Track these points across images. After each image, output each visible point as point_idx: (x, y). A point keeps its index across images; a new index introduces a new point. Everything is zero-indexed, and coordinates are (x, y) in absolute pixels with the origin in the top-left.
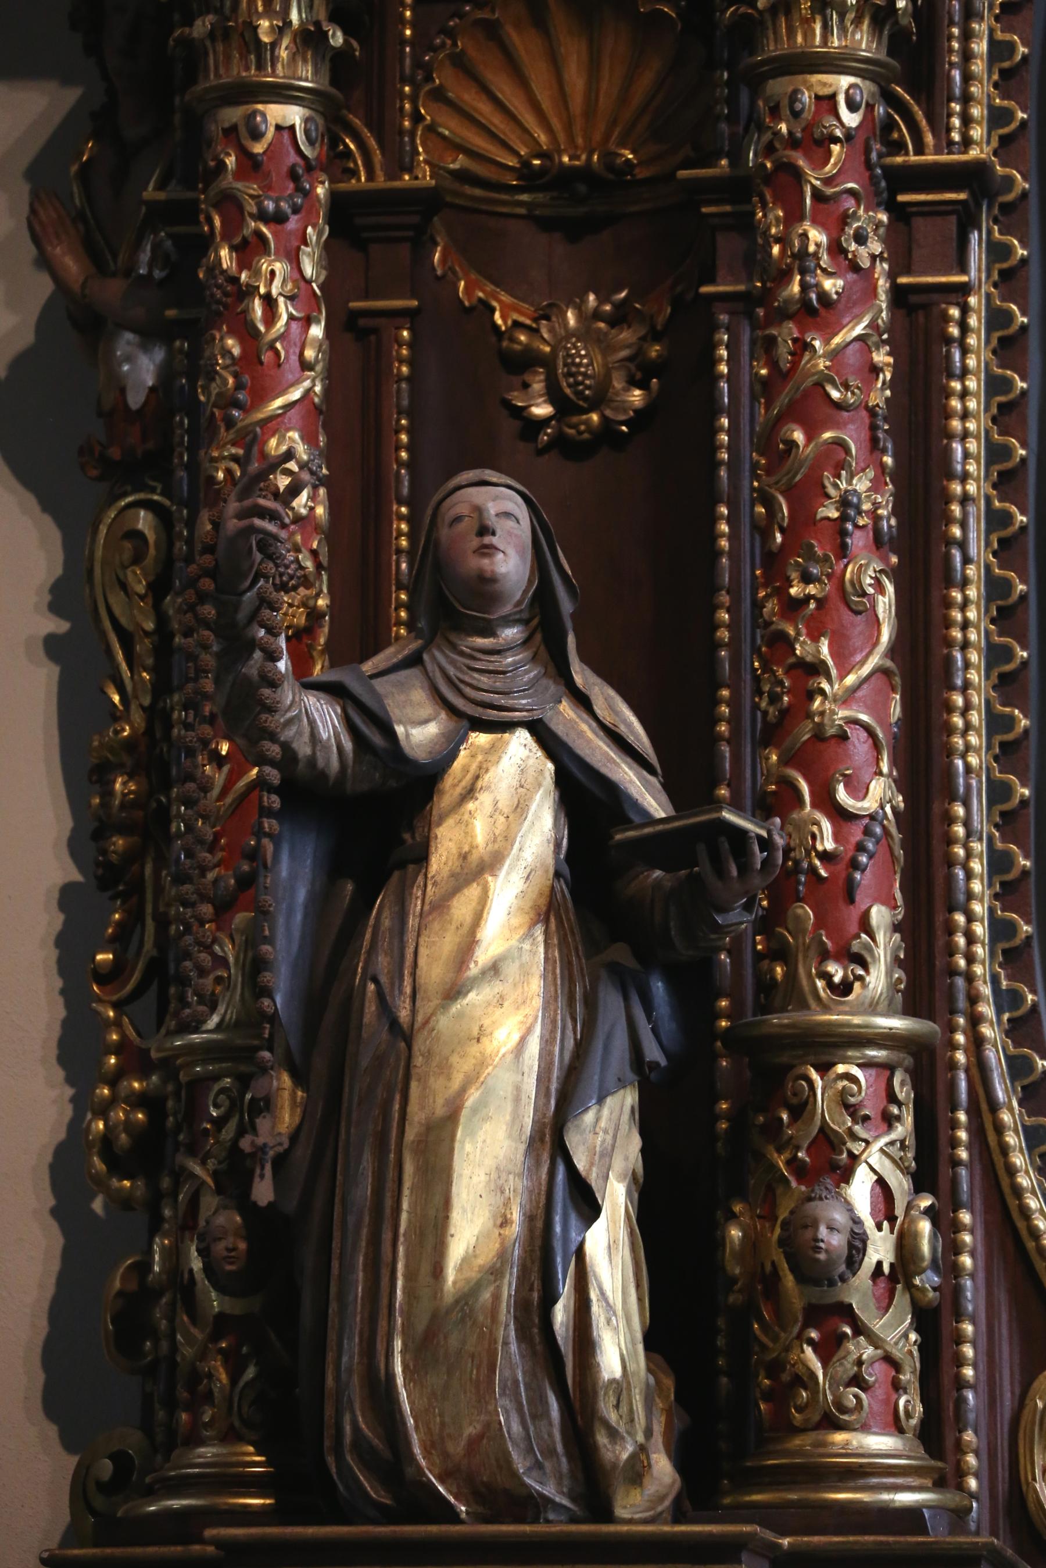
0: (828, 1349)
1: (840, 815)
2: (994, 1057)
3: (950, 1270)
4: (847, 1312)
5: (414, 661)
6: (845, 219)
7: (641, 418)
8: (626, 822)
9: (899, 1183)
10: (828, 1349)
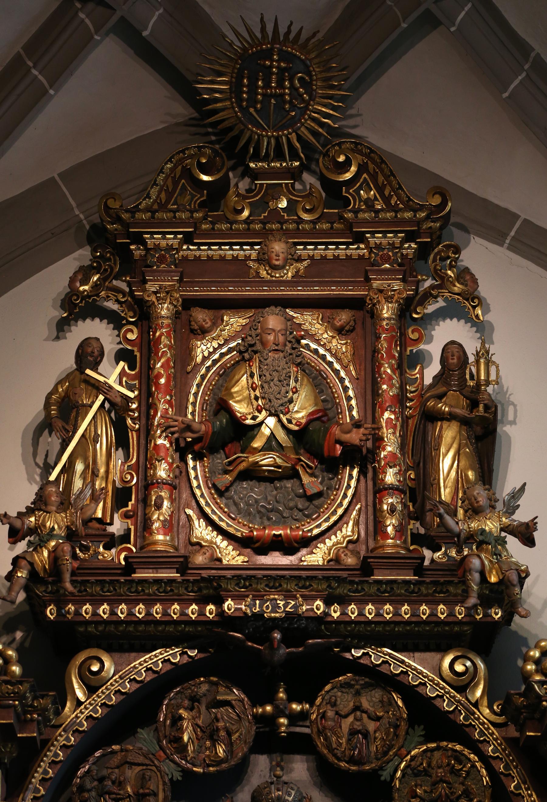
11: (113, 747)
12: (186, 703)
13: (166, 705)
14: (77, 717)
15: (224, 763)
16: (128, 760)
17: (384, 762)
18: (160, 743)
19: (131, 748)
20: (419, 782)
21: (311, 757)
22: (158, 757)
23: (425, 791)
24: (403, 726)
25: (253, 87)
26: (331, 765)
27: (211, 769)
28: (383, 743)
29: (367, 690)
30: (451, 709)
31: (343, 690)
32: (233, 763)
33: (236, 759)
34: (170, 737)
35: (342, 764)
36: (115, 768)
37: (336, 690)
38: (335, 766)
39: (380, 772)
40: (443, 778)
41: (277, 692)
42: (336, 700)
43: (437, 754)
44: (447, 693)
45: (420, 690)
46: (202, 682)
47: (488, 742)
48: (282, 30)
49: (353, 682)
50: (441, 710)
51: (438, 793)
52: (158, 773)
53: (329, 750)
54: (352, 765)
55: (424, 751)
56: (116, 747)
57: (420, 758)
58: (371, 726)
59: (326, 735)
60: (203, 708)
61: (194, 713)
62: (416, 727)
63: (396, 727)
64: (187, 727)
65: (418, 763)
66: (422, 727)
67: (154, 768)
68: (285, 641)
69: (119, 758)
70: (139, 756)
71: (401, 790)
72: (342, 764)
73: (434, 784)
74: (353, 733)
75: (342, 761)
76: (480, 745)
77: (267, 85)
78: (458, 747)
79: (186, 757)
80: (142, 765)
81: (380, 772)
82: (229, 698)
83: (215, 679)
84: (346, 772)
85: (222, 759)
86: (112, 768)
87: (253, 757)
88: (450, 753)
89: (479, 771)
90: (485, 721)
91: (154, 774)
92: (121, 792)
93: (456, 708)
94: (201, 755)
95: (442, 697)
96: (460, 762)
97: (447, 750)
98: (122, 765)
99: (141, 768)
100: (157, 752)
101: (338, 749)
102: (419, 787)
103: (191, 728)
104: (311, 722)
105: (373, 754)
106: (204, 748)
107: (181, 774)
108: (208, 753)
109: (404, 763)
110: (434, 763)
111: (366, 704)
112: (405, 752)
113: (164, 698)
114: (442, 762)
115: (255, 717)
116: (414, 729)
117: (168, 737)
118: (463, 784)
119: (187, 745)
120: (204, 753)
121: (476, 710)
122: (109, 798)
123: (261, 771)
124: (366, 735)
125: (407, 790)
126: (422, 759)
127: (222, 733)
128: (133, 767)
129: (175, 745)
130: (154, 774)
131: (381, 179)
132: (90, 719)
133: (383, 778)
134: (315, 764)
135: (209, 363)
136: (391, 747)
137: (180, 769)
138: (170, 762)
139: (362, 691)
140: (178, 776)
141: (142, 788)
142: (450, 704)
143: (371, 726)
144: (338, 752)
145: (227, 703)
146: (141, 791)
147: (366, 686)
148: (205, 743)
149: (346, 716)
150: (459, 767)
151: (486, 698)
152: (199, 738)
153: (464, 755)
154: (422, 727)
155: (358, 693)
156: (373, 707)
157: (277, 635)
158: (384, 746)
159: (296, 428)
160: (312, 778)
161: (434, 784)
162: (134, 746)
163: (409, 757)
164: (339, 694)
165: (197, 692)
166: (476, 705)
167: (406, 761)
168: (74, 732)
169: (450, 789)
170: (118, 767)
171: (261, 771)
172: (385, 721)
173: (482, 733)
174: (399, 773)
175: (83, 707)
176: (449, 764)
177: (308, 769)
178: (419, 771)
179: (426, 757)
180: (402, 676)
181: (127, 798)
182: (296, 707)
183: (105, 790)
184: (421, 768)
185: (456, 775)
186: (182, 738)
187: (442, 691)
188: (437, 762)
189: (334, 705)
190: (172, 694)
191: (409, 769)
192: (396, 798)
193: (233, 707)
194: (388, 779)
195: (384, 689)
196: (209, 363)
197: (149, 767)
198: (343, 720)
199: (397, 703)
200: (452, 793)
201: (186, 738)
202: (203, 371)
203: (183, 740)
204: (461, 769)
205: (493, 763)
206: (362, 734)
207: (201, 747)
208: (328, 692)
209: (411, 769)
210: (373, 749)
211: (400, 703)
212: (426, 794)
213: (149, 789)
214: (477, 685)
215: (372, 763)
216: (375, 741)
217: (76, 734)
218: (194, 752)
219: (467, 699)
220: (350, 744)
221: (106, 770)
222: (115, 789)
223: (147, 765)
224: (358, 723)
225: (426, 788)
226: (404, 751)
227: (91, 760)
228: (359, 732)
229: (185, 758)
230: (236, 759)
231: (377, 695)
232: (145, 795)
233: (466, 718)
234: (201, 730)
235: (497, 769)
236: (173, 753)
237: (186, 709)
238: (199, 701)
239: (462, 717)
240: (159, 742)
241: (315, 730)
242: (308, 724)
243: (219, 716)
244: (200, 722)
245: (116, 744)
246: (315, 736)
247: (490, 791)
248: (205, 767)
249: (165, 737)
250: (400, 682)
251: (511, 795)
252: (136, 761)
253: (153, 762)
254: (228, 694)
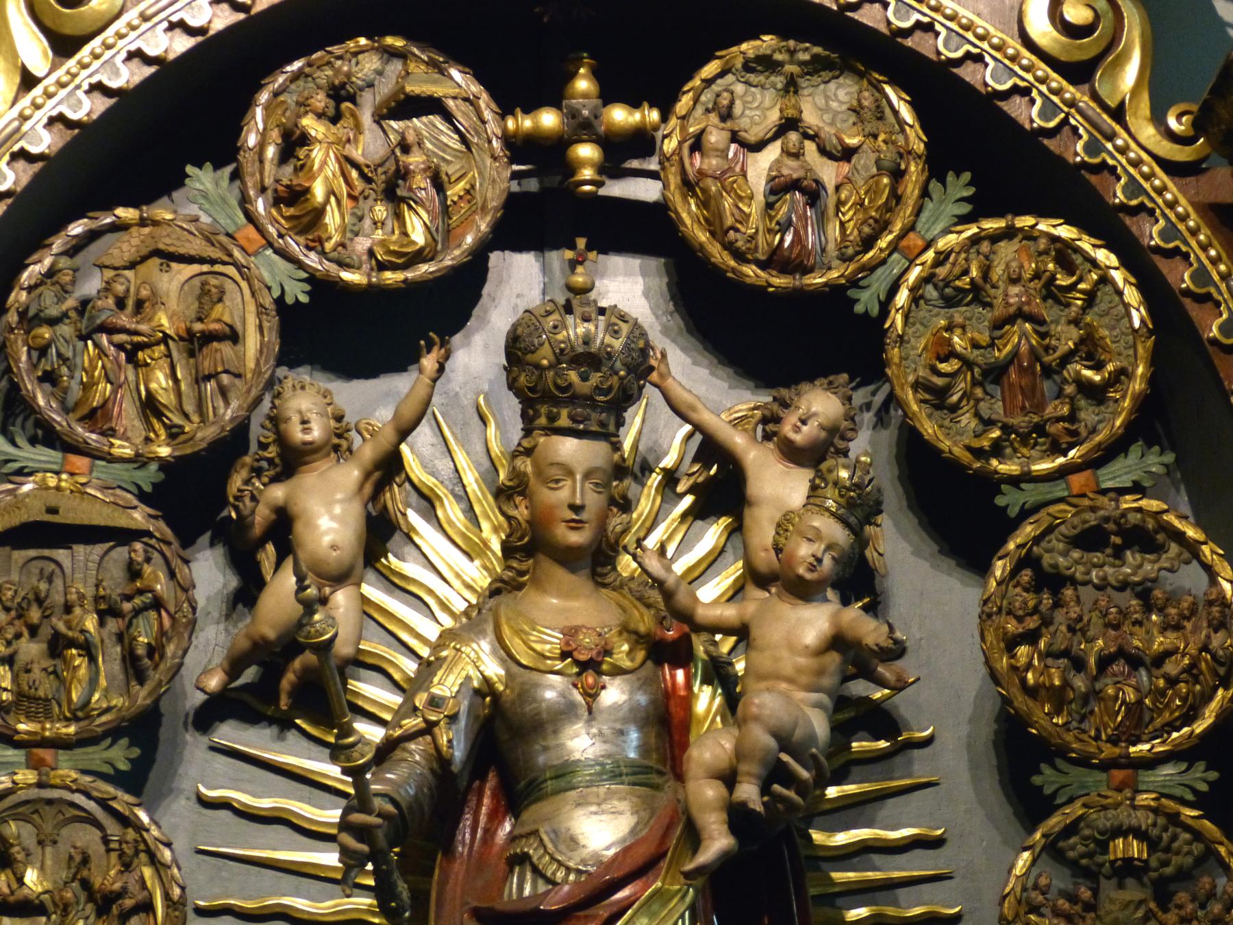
11: (120, 212)
12: (320, 100)
13: (267, 108)
14: (24, 118)
15: (425, 261)
16: (161, 246)
17: (862, 268)
18: (248, 206)
19: (169, 216)
20: (958, 319)
21: (655, 263)
22: (243, 242)
23: (975, 345)
24: (915, 171)
26: (717, 272)
27: (388, 275)
28: (861, 216)
29: (816, 79)
30: (1052, 124)
31: (752, 77)
32: (448, 262)
33: (457, 252)
34: (276, 191)
35: (750, 271)
36: (125, 268)
37: (730, 78)
38: (730, 275)
39: (851, 293)
40: (1026, 308)
41: (573, 75)
42: (732, 103)
43: (1007, 250)
44: (1042, 81)
45: (967, 73)
46: (362, 51)
47: (1151, 212)
49: (778, 57)
50: (1020, 127)
51: (1009, 348)
52: (244, 284)
53: (713, 234)
54: (774, 273)
55: (975, 240)
56: (126, 213)
57: (963, 255)
58: (829, 173)
59: (705, 191)
60: (366, 118)
61: (343, 129)
62: (950, 177)
63: (898, 175)
64: (324, 163)
65: (957, 270)
66: (967, 176)
67: (231, 270)
69: (135, 241)
70: (191, 237)
71: (908, 342)
72: (750, 271)
73: (998, 325)
74: (779, 188)
75: (748, 262)
76: (1128, 221)
78: (1066, 232)
79: (320, 241)
80: (201, 261)
81: (850, 293)
82: (438, 90)
83: (399, 43)
84: (759, 292)
85: (422, 250)
86: (116, 269)
87: (495, 258)
88: (1043, 243)
89: (1120, 293)
90: (1145, 156)
91: (234, 285)
92: (143, 327)
93: (1065, 122)
94: (359, 239)
95: (1025, 92)
96: (1069, 268)
97: (1035, 239)
98: (144, 259)
99: (196, 268)
100: (239, 229)
101: (737, 230)
102: (958, 331)
103: (333, 166)
104: (665, 160)
105: (831, 247)
106: (367, 223)
107: (307, 287)
108: (379, 235)
109: (919, 269)
110: (998, 272)
111: (810, 118)
112: (920, 243)
113: (259, 87)
114: (1021, 267)
115: (509, 140)
116: (943, 181)
117: (270, 192)
118: (1076, 322)
119: (320, 212)
120: (368, 236)
121: (1118, 128)
122: (111, 342)
123: (518, 296)
124: (814, 194)
125: (923, 342)
126: (966, 259)
127: (421, 182)
128: (174, 265)
129: (291, 211)
130: (229, 285)
132: (59, 126)
133: (859, 308)
134: (666, 280)
136: (882, 226)
137: (305, 275)
138: (276, 257)
139: (803, 82)
140: (298, 292)
141: (200, 320)
142: (1049, 110)
143: (829, 173)
144: (738, 236)
145: (433, 106)
146: (198, 327)
147: (816, 67)
148: (371, 210)
149: (758, 147)
150: (1063, 281)
151: (1145, 97)
152: (356, 193)
153: (1078, 250)
154: (967, 176)
155: (792, 86)
156: (832, 124)
158: (864, 222)
160: (657, 317)
161: (998, 325)
162: (175, 212)
163: (930, 255)
164: (739, 88)
165: (349, 75)
166: (1118, 114)
167: (922, 264)
168: (15, 157)
169: (1043, 336)
170: (132, 266)
171: (518, 296)
172: (865, 162)
173: (1134, 188)
174: (902, 297)
175: (37, 91)
176: (1037, 276)
177: (646, 294)
178: (958, 290)
179: (978, 253)
180: (918, 35)
181: (158, 343)
182: (620, 116)
183: (99, 321)
184: (964, 283)
185: (1058, 302)
186: (307, 190)
187: (1029, 77)
188: (1008, 266)
189: (726, 115)
190: (281, 80)
191: (930, 288)
192: (896, 360)
193: (448, 117)
194: (875, 311)
195: (861, 75)
197: (218, 268)
198: (752, 157)
199: (896, 113)
200: (1047, 349)
201: (319, 191)
203: (314, 196)
204: (1072, 287)
205: (1162, 264)
206: (803, 191)
207: (361, 219)
208: (708, 82)
209: (936, 287)
210: (834, 231)
211: (906, 113)
212: (976, 352)
213: (219, 320)
214: (1123, 58)
215: (830, 269)
216: (838, 210)
217: (21, 164)
218: (343, 229)
219: (1095, 97)
220: (771, 218)
221: (98, 270)
222: (124, 320)
223: (213, 262)
224: (792, 163)
225: (977, 336)
226: (914, 240)
227: (58, 244)
228: (794, 185)
229: (317, 245)
230: (457, 252)
231: (842, 94)
232: (209, 338)
233: (1093, 147)
234: (362, 175)
235: (1171, 279)
236: (283, 231)
237: (320, 116)
238: (352, 99)
239: (1079, 146)
240: (244, 201)
241: (674, 180)
242: (653, 165)
243: (411, 138)
244: (357, 154)
245: (126, 205)
246: (676, 199)
247: (1150, 343)
248: (372, 269)
249: (263, 190)
250: (913, 54)
251: (1210, 349)
252: (182, 251)
253: (230, 255)
254: (435, 82)
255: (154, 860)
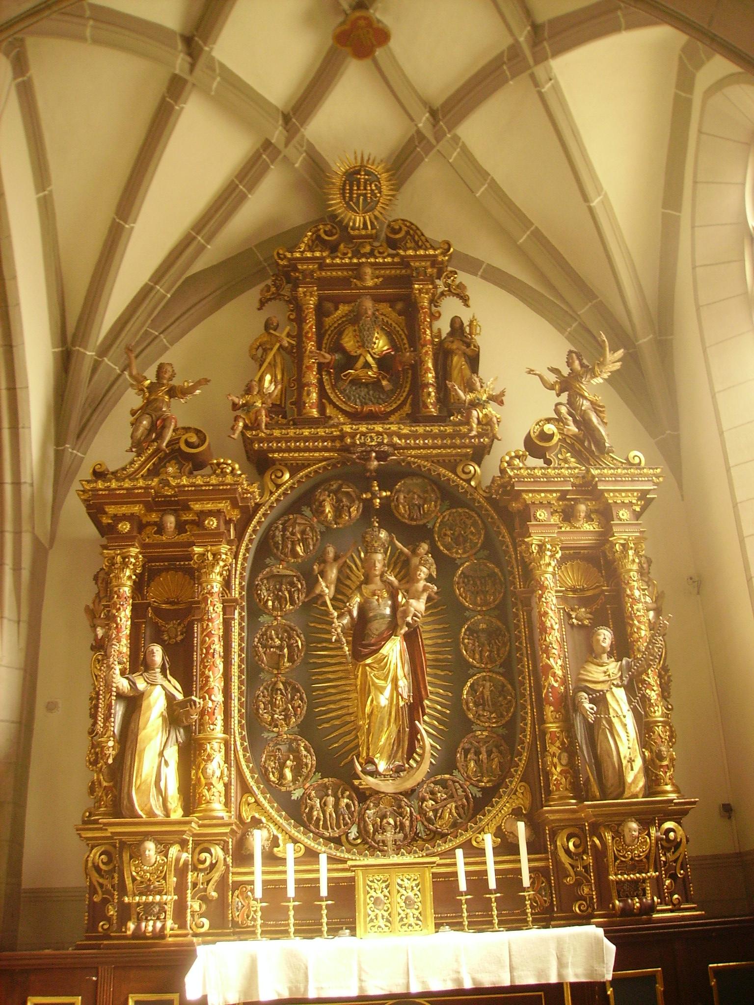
0: (209, 790)
1: (213, 701)
2: (238, 743)
3: (230, 777)
4: (212, 784)
5: (141, 675)
6: (215, 605)
7: (182, 640)
8: (175, 700)
9: (222, 763)
10: (209, 790)
25: (351, 190)
48: (366, 158)
68: (377, 458)
77: (358, 189)
131: (416, 238)
135: (332, 328)
157: (374, 454)
159: (378, 357)
182: (384, 494)
196: (332, 328)
202: (329, 332)
255: (299, 637)
